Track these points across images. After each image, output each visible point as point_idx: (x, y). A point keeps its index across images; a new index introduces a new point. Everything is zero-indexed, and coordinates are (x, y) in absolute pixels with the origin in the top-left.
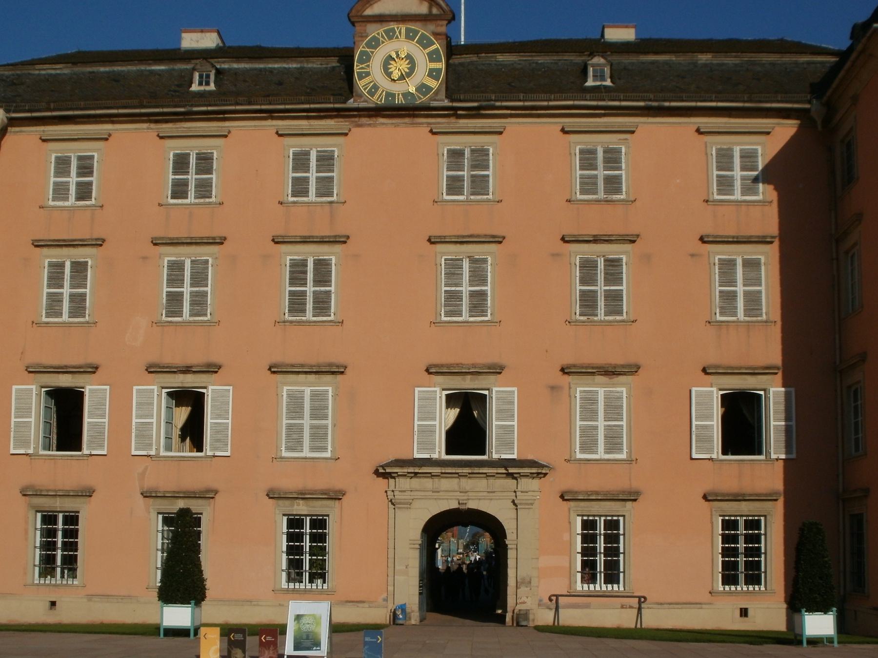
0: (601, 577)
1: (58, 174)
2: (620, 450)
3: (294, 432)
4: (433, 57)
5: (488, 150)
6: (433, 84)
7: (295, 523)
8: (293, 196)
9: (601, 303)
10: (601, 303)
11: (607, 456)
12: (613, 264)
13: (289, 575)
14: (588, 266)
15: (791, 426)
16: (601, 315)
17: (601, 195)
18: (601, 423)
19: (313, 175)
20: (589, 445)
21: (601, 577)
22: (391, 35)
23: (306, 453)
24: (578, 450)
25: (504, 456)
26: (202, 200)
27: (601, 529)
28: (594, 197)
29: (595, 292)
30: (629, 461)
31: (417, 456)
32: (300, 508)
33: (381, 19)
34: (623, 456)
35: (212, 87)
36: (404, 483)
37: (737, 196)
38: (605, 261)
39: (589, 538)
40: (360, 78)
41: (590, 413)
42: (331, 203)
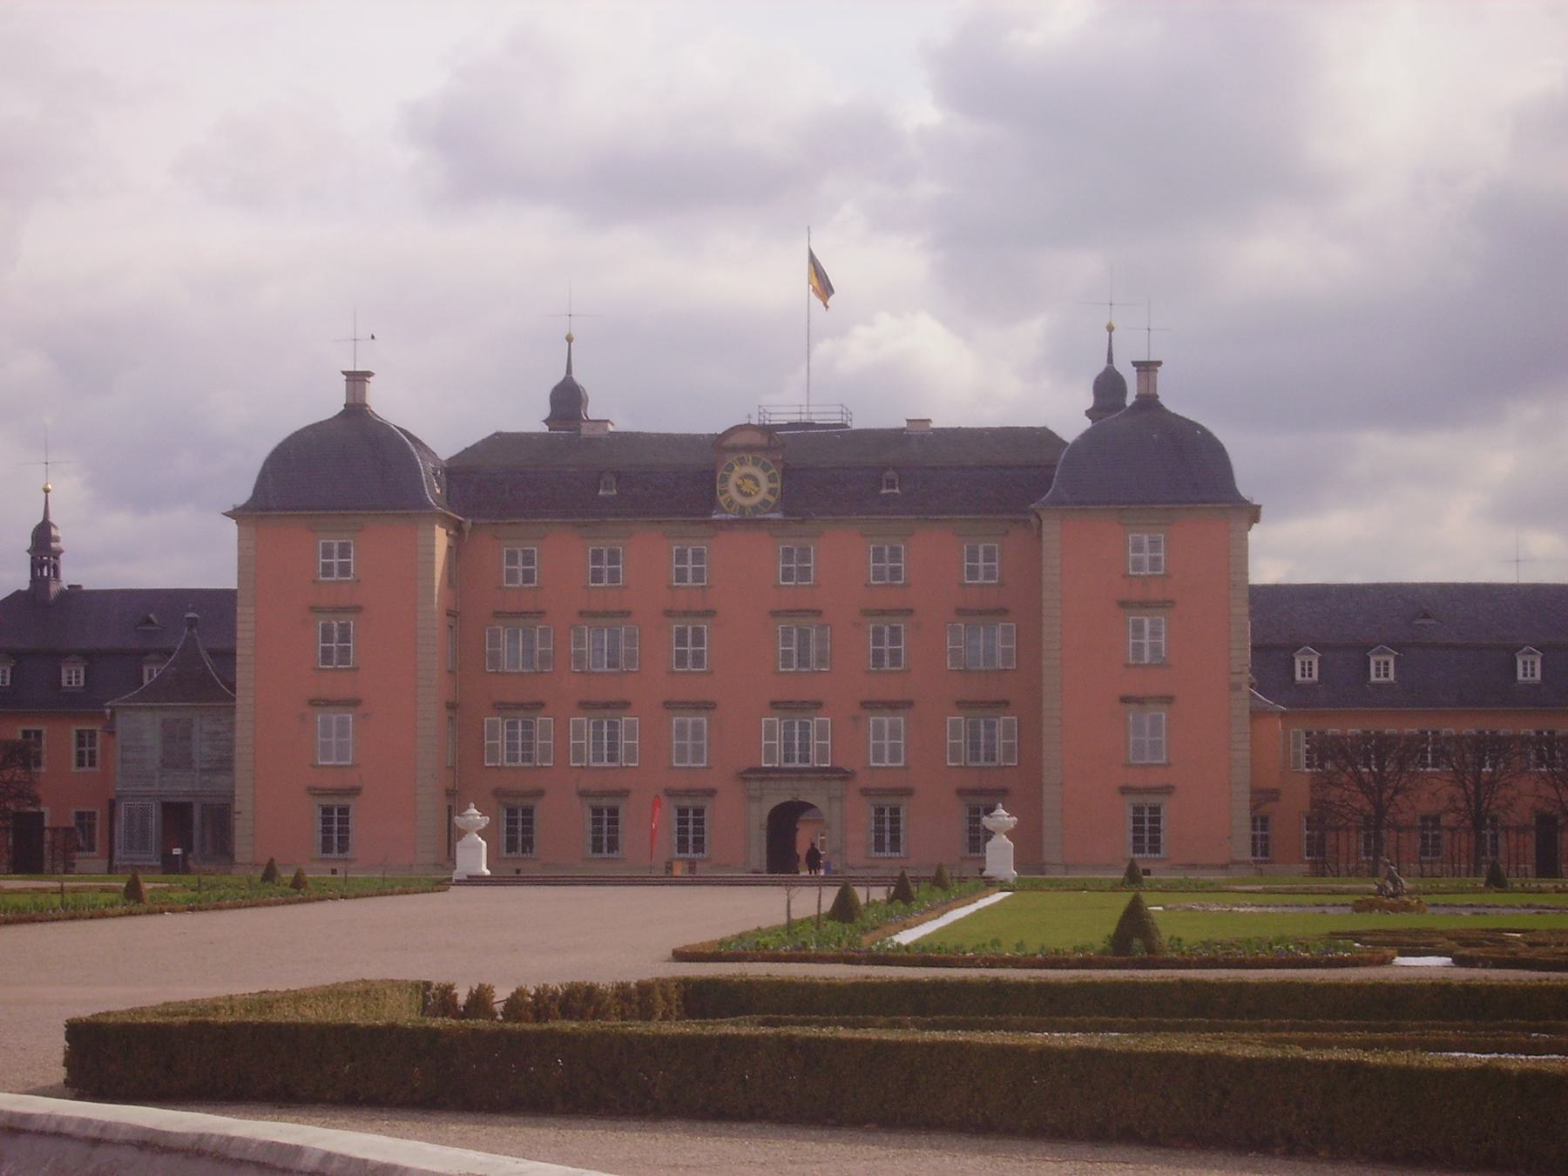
0: (887, 848)
1: (508, 563)
2: (899, 761)
3: (681, 748)
4: (771, 479)
5: (810, 549)
6: (772, 499)
7: (682, 812)
8: (677, 581)
9: (887, 658)
10: (887, 658)
11: (890, 764)
12: (895, 631)
13: (679, 848)
14: (878, 632)
15: (1012, 746)
16: (887, 666)
17: (888, 581)
18: (886, 742)
19: (690, 566)
20: (878, 758)
21: (887, 848)
22: (742, 462)
23: (689, 764)
24: (871, 761)
25: (821, 765)
26: (613, 585)
27: (887, 814)
28: (883, 582)
29: (883, 650)
30: (906, 768)
31: (764, 765)
32: (687, 802)
33: (735, 449)
34: (901, 764)
35: (615, 492)
36: (755, 785)
37: (981, 580)
38: (890, 627)
39: (879, 821)
40: (721, 494)
41: (879, 735)
42: (703, 586)
